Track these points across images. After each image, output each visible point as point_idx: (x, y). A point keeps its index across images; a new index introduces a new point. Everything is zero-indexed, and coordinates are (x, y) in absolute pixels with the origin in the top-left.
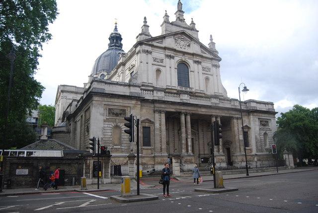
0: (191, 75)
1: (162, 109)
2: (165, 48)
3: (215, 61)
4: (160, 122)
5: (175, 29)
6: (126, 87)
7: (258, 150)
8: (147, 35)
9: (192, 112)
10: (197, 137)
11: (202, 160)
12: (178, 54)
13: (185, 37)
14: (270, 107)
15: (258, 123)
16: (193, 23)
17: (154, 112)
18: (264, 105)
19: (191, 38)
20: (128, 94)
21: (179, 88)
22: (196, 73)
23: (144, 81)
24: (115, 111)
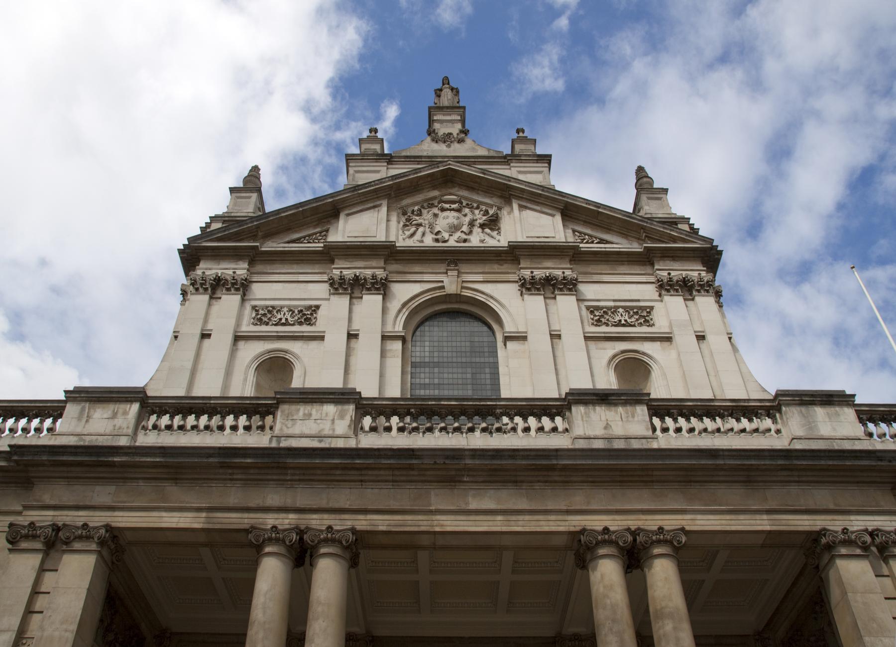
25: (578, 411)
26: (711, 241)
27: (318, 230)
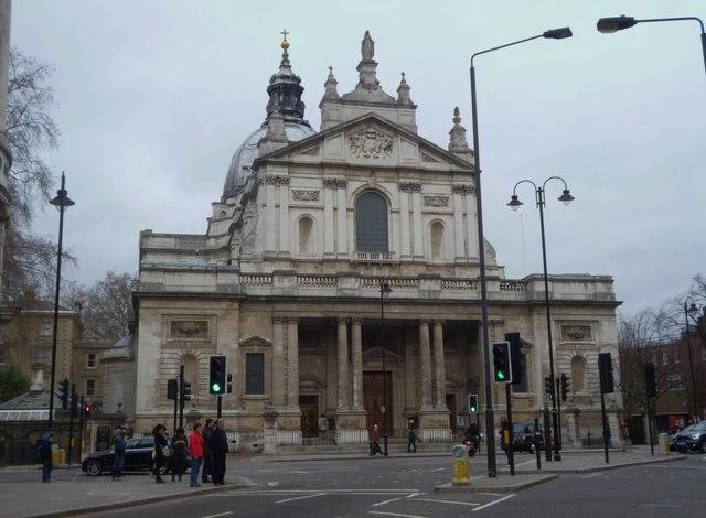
0: (393, 221)
1: (289, 315)
2: (322, 166)
3: (462, 178)
4: (284, 342)
5: (350, 113)
6: (208, 276)
8: (277, 141)
9: (365, 315)
12: (358, 173)
14: (600, 288)
16: (404, 88)
17: (273, 322)
18: (582, 285)
19: (395, 130)
20: (212, 289)
22: (405, 215)
23: (269, 249)
24: (186, 327)
25: (422, 281)
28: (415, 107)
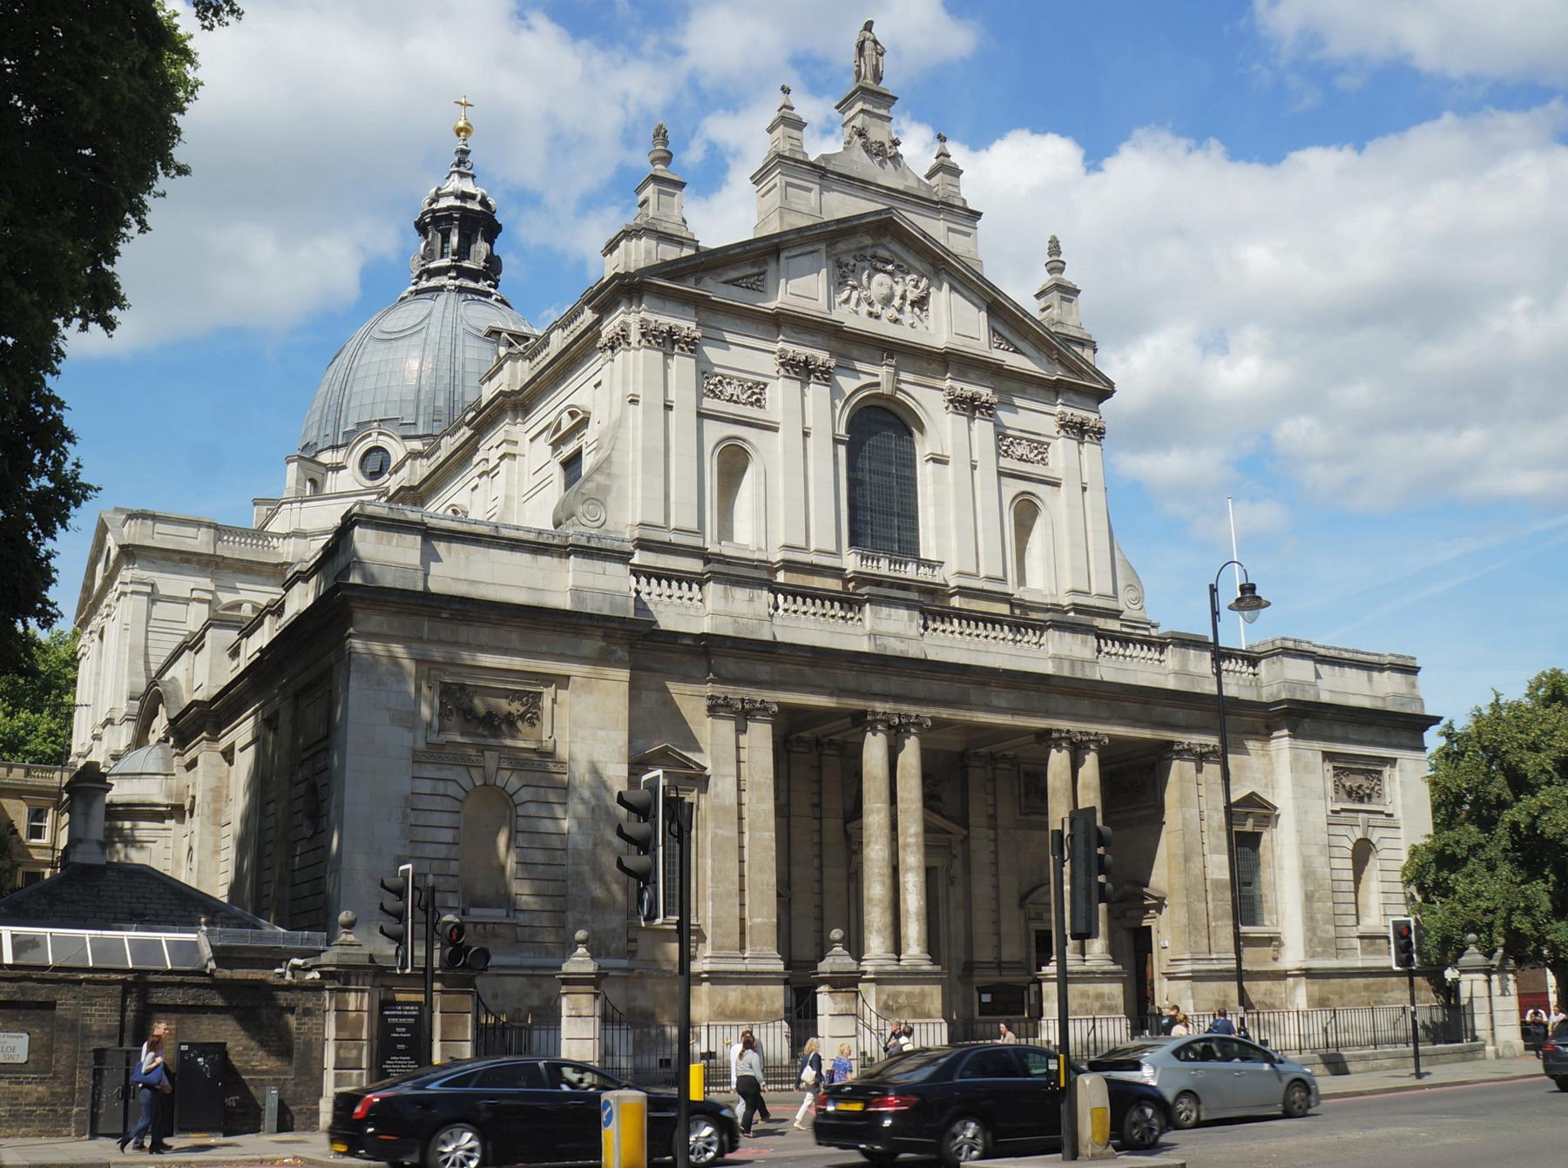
7: (1314, 941)
10: (957, 863)
11: (986, 998)
13: (895, 247)
15: (1322, 777)
18: (1363, 674)
21: (851, 562)
26: (1111, 384)
27: (755, 270)
28: (976, 215)
